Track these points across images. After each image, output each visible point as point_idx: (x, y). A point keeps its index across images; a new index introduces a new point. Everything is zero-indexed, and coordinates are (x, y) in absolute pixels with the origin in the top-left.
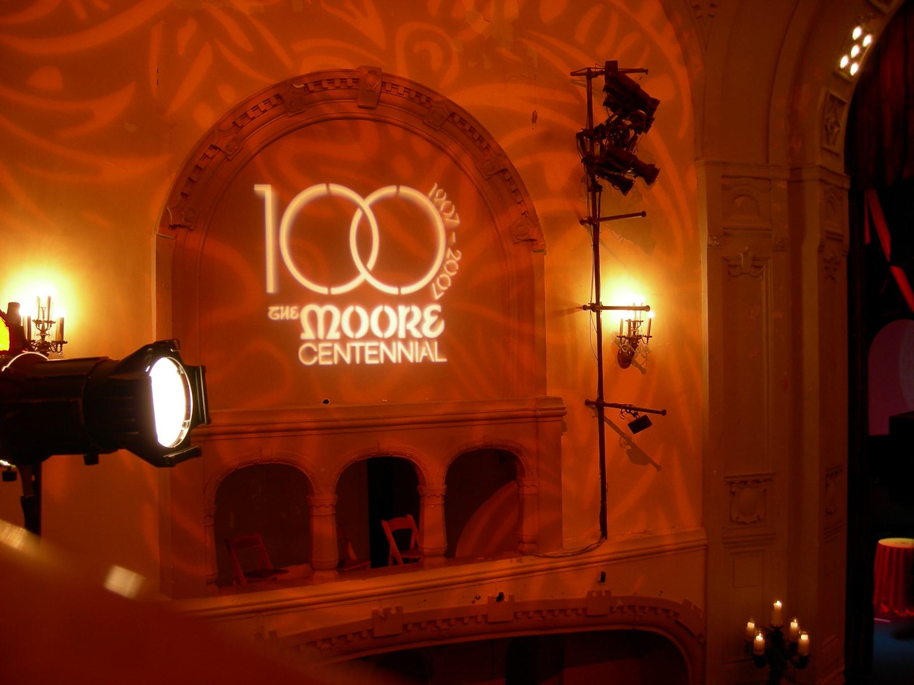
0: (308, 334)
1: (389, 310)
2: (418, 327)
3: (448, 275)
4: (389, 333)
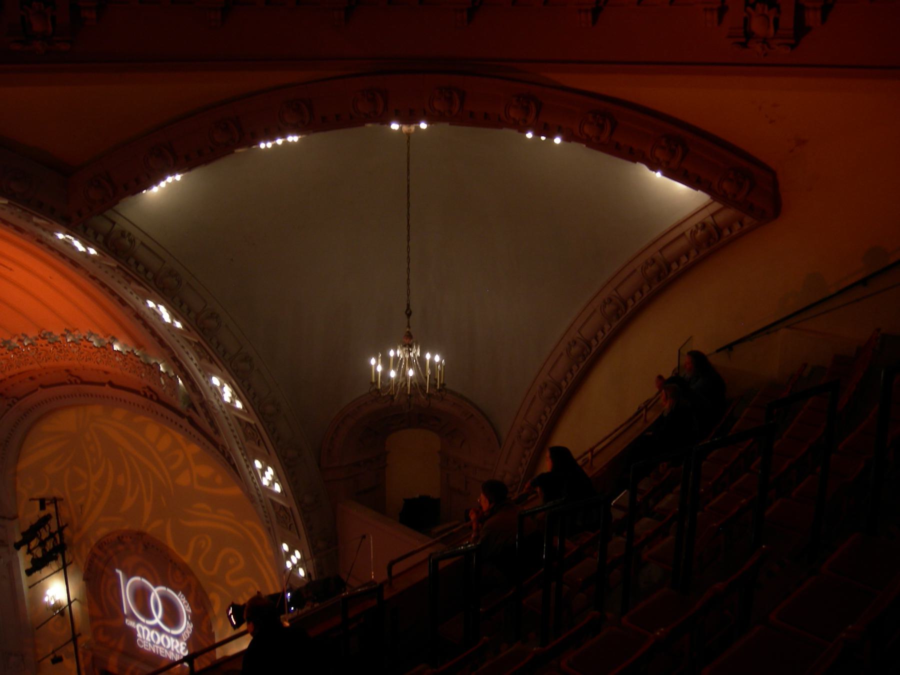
0: (139, 635)
1: (167, 638)
2: (179, 648)
3: (189, 633)
4: (168, 647)
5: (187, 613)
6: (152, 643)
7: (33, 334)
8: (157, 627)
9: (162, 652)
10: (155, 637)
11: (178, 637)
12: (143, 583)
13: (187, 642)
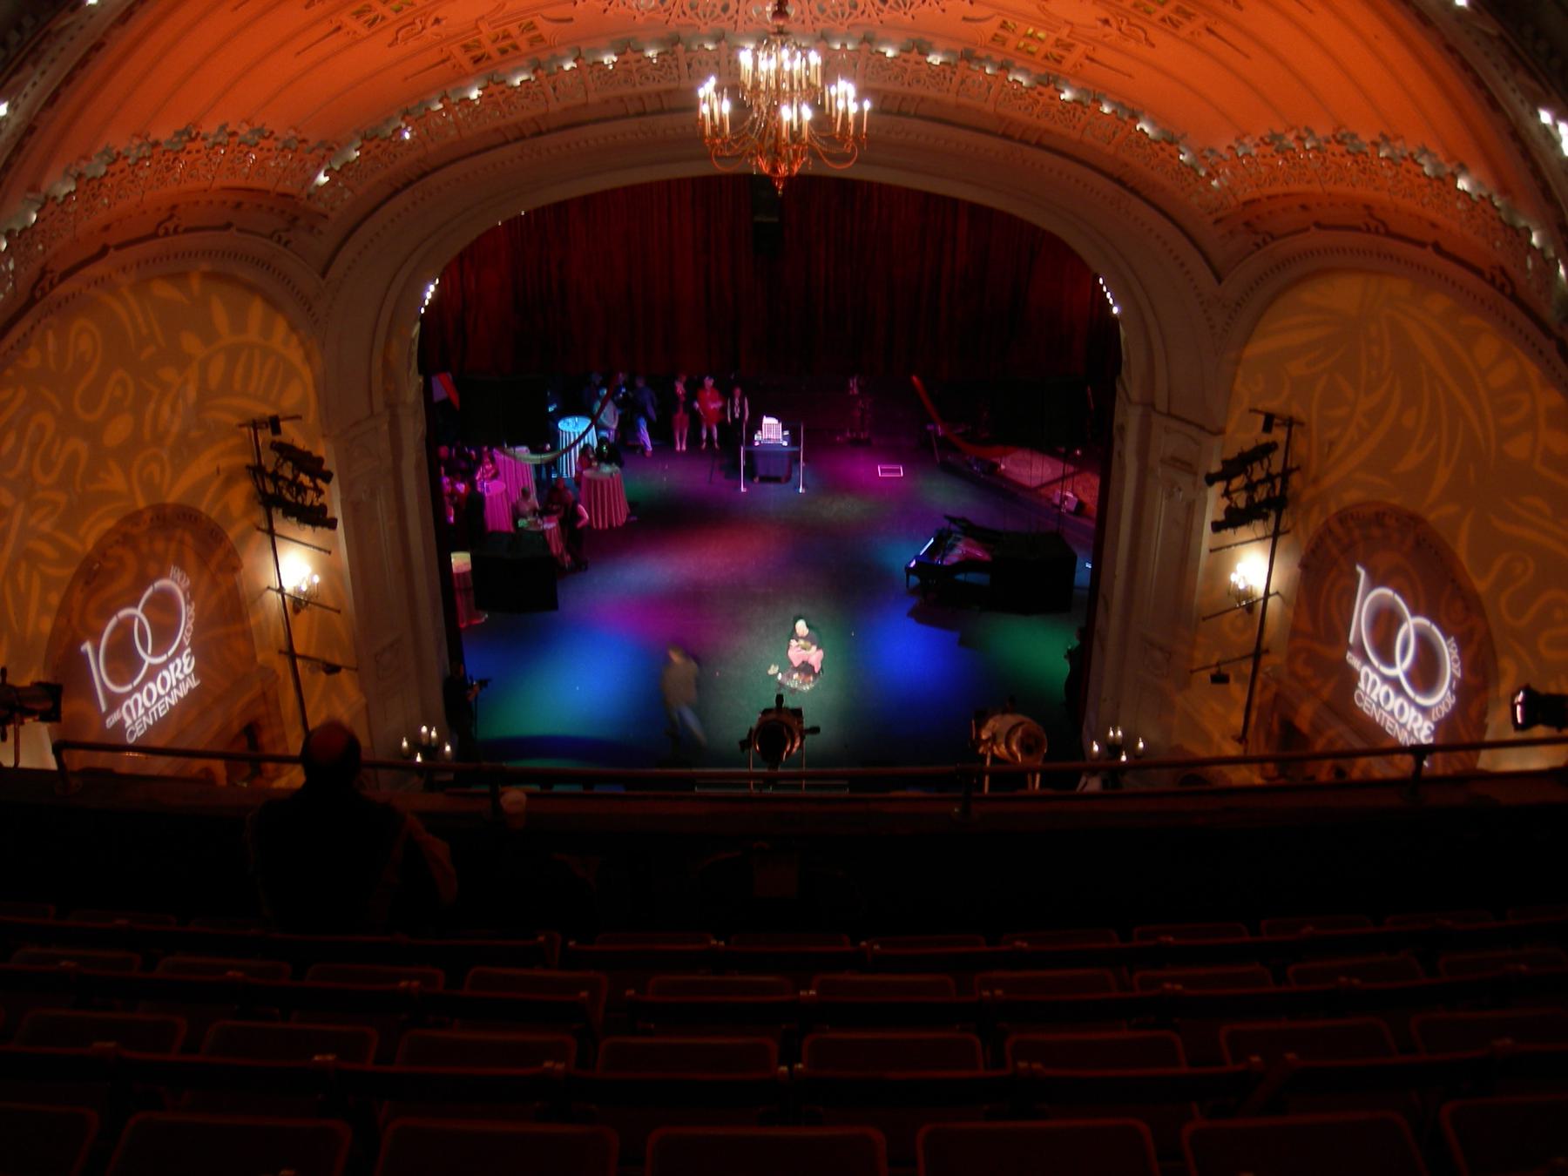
0: (1361, 685)
1: (1406, 705)
2: (1420, 730)
3: (1445, 710)
4: (1403, 720)
5: (1453, 677)
6: (1378, 705)
7: (1323, 131)
8: (1395, 683)
9: (1390, 725)
10: (1387, 697)
11: (1425, 710)
12: (1396, 603)
13: (1438, 724)
